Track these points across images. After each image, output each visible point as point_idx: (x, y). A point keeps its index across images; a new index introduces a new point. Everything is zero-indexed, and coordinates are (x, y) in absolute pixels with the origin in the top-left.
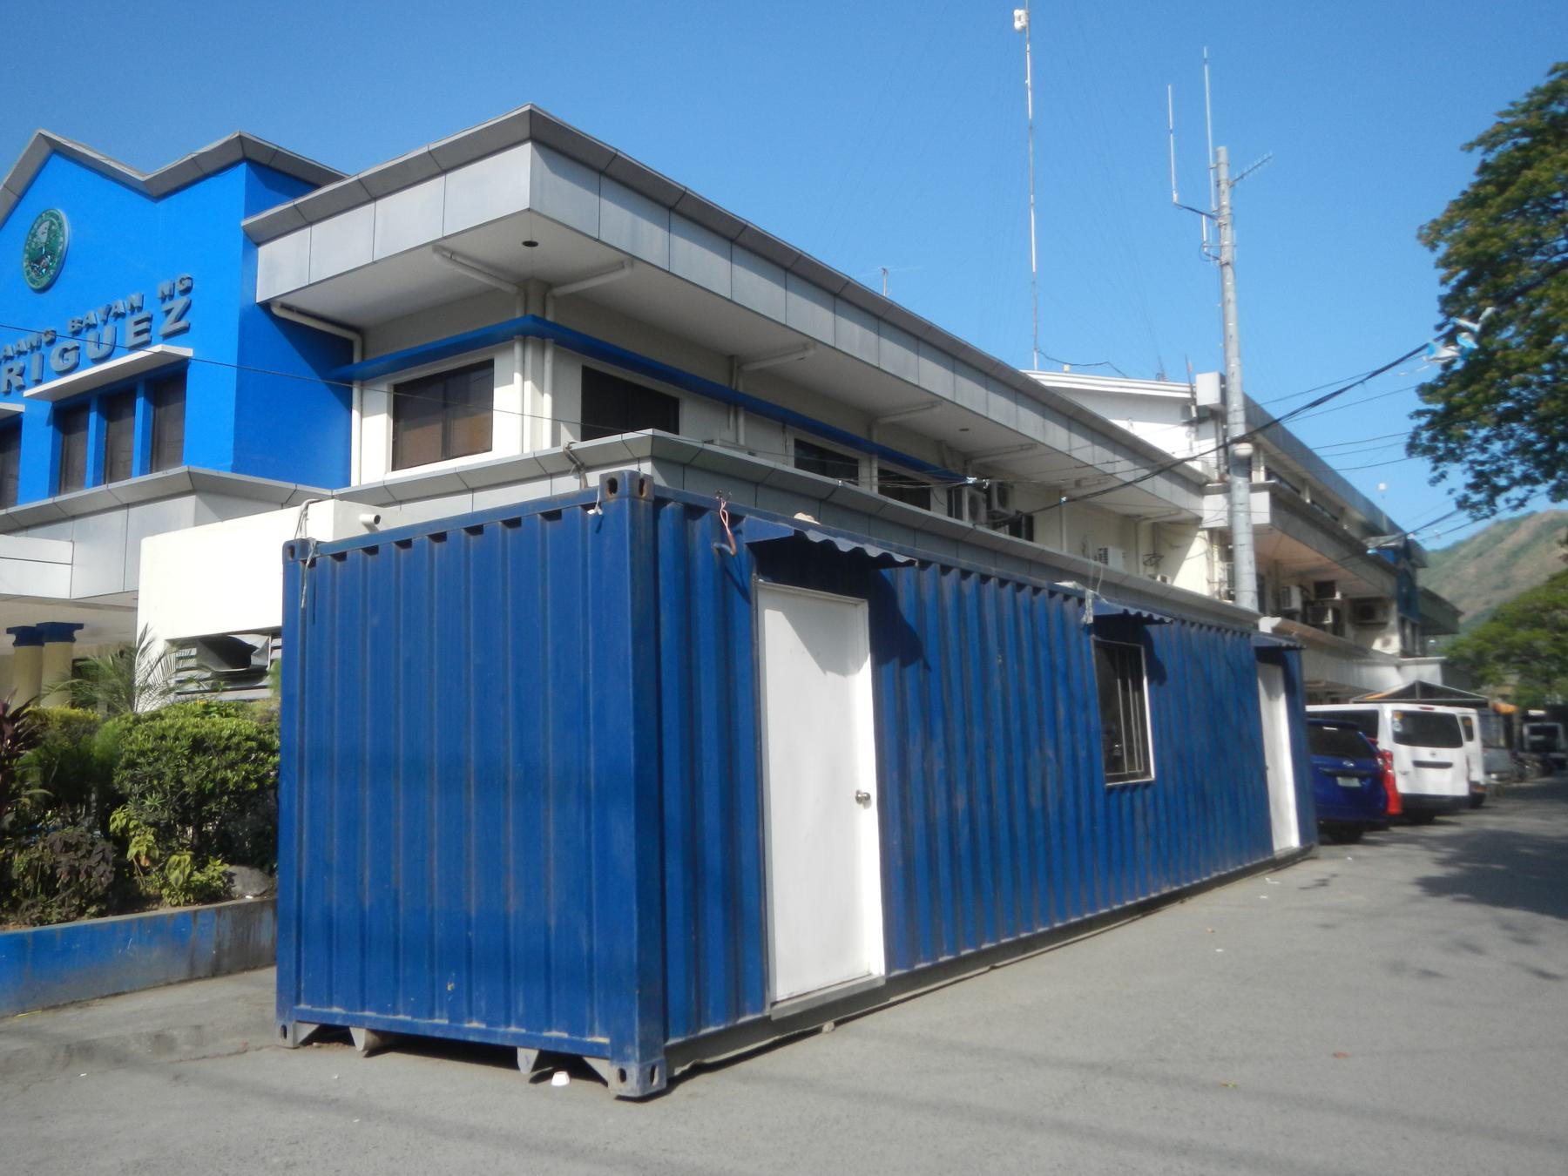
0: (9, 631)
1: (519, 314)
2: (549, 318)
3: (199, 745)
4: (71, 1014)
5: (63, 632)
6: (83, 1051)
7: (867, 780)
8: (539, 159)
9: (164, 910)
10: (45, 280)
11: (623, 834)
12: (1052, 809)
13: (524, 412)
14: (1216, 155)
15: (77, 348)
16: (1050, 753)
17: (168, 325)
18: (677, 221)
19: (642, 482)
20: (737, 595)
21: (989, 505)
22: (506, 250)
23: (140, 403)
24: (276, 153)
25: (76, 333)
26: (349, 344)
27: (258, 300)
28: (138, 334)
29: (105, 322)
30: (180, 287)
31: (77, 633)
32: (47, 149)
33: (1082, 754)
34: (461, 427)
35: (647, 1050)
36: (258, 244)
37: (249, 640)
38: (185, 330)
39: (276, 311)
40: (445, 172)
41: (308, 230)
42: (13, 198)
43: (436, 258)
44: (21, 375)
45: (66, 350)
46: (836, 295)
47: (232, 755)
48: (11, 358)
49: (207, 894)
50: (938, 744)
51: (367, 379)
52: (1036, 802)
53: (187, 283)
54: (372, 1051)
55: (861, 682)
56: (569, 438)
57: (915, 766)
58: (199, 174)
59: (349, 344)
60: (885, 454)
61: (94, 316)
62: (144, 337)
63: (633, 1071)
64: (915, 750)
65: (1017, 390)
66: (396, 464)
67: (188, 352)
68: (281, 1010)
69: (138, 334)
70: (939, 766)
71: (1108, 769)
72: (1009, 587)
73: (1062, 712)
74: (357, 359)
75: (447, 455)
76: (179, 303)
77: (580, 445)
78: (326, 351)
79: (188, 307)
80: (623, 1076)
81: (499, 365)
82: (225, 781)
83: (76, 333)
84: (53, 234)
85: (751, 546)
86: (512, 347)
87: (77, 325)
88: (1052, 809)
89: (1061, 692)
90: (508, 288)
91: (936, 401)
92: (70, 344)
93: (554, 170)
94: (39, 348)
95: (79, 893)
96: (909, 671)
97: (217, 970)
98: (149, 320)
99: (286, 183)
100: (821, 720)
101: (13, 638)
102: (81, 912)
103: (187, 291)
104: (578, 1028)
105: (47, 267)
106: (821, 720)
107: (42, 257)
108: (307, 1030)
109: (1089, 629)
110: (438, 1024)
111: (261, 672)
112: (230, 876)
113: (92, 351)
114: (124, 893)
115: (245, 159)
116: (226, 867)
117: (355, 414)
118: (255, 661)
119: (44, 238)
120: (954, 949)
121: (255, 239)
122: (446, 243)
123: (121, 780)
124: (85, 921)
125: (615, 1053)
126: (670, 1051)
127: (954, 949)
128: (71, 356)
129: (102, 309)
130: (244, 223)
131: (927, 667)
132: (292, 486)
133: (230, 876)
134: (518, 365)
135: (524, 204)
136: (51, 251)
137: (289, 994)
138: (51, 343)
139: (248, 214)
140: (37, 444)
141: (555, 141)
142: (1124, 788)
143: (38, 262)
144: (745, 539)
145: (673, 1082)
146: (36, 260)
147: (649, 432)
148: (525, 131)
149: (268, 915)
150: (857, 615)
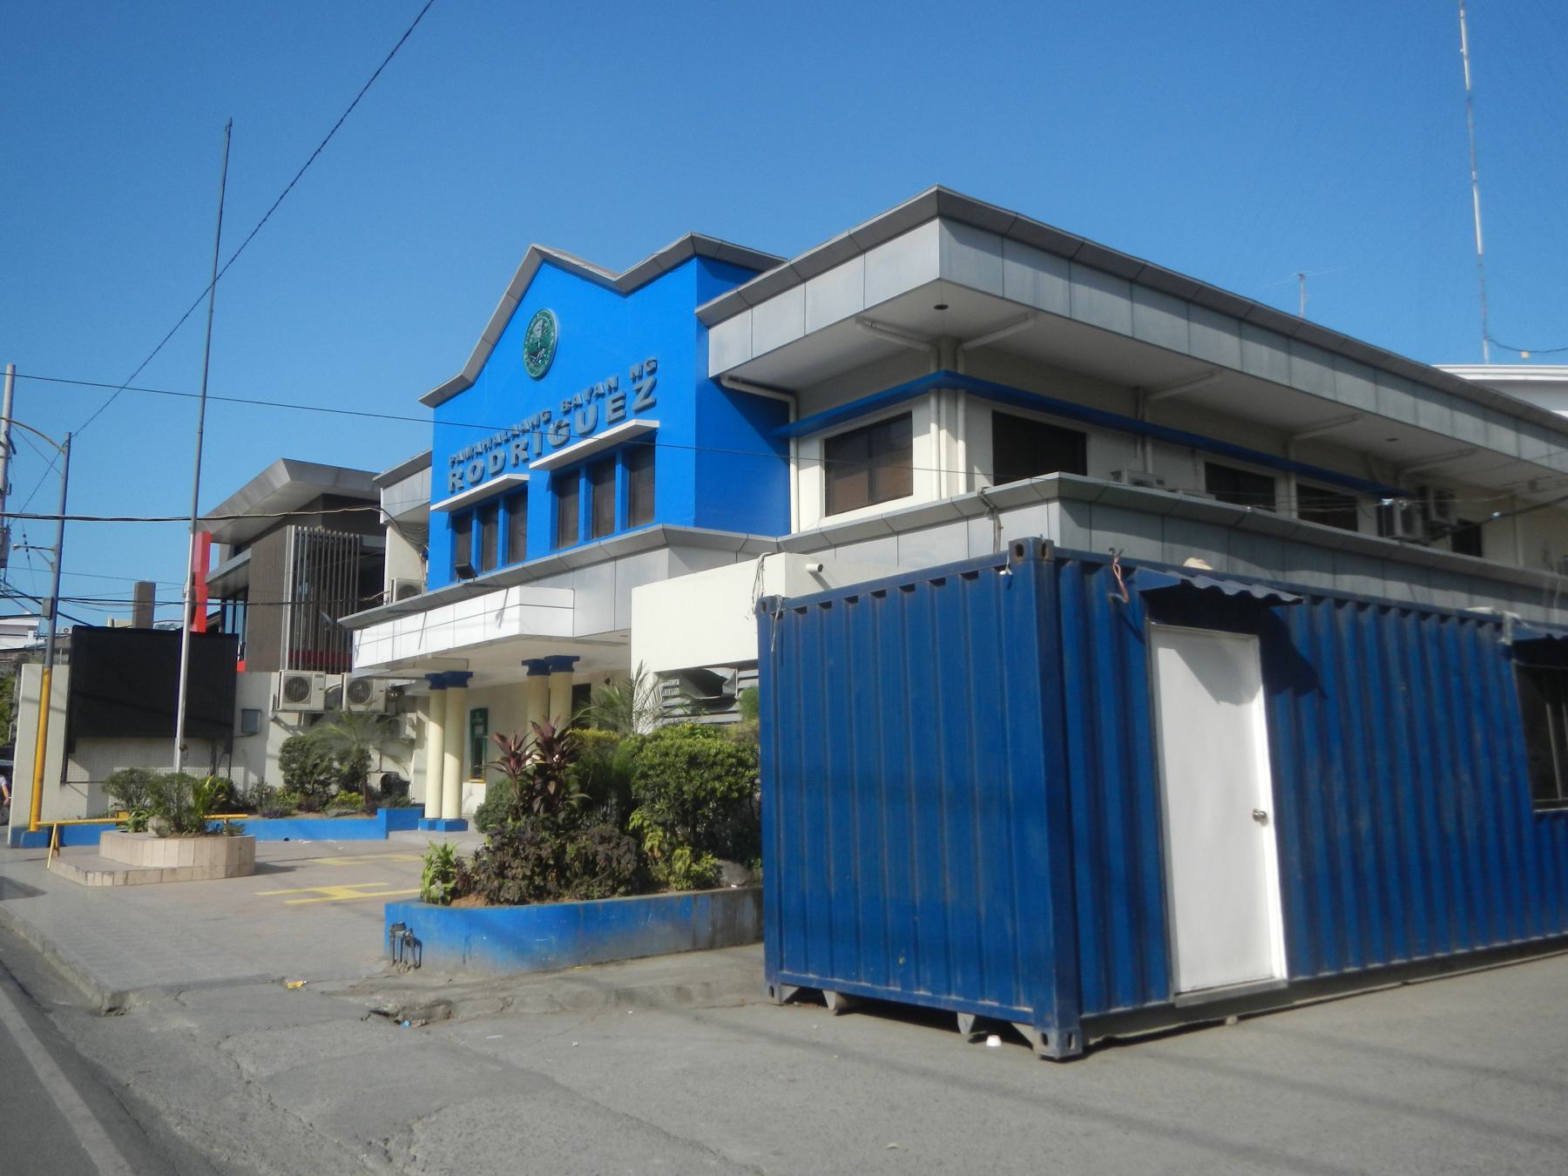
0: (524, 663)
1: (933, 370)
2: (961, 371)
3: (693, 761)
4: (612, 969)
5: (564, 664)
6: (626, 996)
7: (1265, 801)
9: (672, 893)
10: (541, 370)
11: (1038, 839)
12: (1470, 832)
13: (940, 459)
16: (1466, 778)
17: (639, 402)
18: (1076, 269)
19: (1044, 546)
20: (1132, 638)
21: (1425, 512)
22: (922, 314)
23: (619, 468)
24: (721, 247)
26: (785, 405)
27: (711, 374)
28: (615, 410)
30: (646, 369)
31: (575, 664)
32: (538, 259)
33: (1505, 780)
34: (884, 474)
35: (1064, 1022)
36: (709, 327)
37: (720, 672)
38: (653, 405)
39: (725, 383)
40: (864, 251)
42: (515, 302)
43: (859, 327)
46: (1241, 320)
47: (718, 770)
49: (701, 882)
50: (1337, 767)
51: (802, 436)
52: (1450, 827)
53: (653, 365)
54: (842, 1011)
55: (1256, 711)
56: (983, 482)
57: (1313, 787)
59: (785, 405)
60: (1302, 470)
61: (580, 397)
62: (620, 413)
63: (1053, 1036)
64: (1313, 773)
65: (1450, 394)
66: (830, 510)
67: (655, 424)
68: (768, 975)
69: (615, 410)
70: (1338, 788)
71: (1536, 795)
72: (1411, 618)
73: (1479, 737)
74: (792, 420)
75: (873, 500)
76: (647, 382)
77: (993, 489)
78: (767, 413)
80: (1045, 1040)
81: (917, 417)
82: (714, 790)
83: (567, 412)
84: (546, 331)
85: (1144, 594)
86: (927, 401)
88: (1470, 832)
89: (1477, 719)
90: (923, 347)
91: (1356, 414)
93: (961, 240)
95: (612, 875)
96: (1306, 701)
97: (711, 946)
98: (623, 398)
99: (731, 272)
100: (1217, 749)
101: (526, 668)
102: (614, 891)
103: (653, 372)
104: (1006, 998)
106: (1217, 749)
108: (790, 991)
109: (1508, 652)
110: (893, 990)
111: (730, 700)
112: (719, 868)
113: (580, 427)
114: (642, 881)
115: (696, 255)
116: (716, 861)
117: (793, 467)
118: (726, 690)
120: (1362, 961)
121: (706, 323)
122: (870, 314)
123: (636, 786)
124: (616, 898)
125: (1038, 1021)
126: (1085, 1024)
127: (1362, 961)
128: (563, 431)
129: (587, 390)
131: (1323, 696)
132: (743, 536)
133: (719, 868)
134: (933, 416)
135: (934, 273)
136: (545, 346)
137: (775, 963)
138: (548, 421)
139: (700, 302)
140: (540, 505)
141: (962, 216)
142: (1557, 816)
143: (535, 354)
144: (1137, 588)
145: (1088, 1051)
146: (533, 354)
147: (1055, 475)
148: (933, 209)
149: (749, 903)
150: (1247, 654)
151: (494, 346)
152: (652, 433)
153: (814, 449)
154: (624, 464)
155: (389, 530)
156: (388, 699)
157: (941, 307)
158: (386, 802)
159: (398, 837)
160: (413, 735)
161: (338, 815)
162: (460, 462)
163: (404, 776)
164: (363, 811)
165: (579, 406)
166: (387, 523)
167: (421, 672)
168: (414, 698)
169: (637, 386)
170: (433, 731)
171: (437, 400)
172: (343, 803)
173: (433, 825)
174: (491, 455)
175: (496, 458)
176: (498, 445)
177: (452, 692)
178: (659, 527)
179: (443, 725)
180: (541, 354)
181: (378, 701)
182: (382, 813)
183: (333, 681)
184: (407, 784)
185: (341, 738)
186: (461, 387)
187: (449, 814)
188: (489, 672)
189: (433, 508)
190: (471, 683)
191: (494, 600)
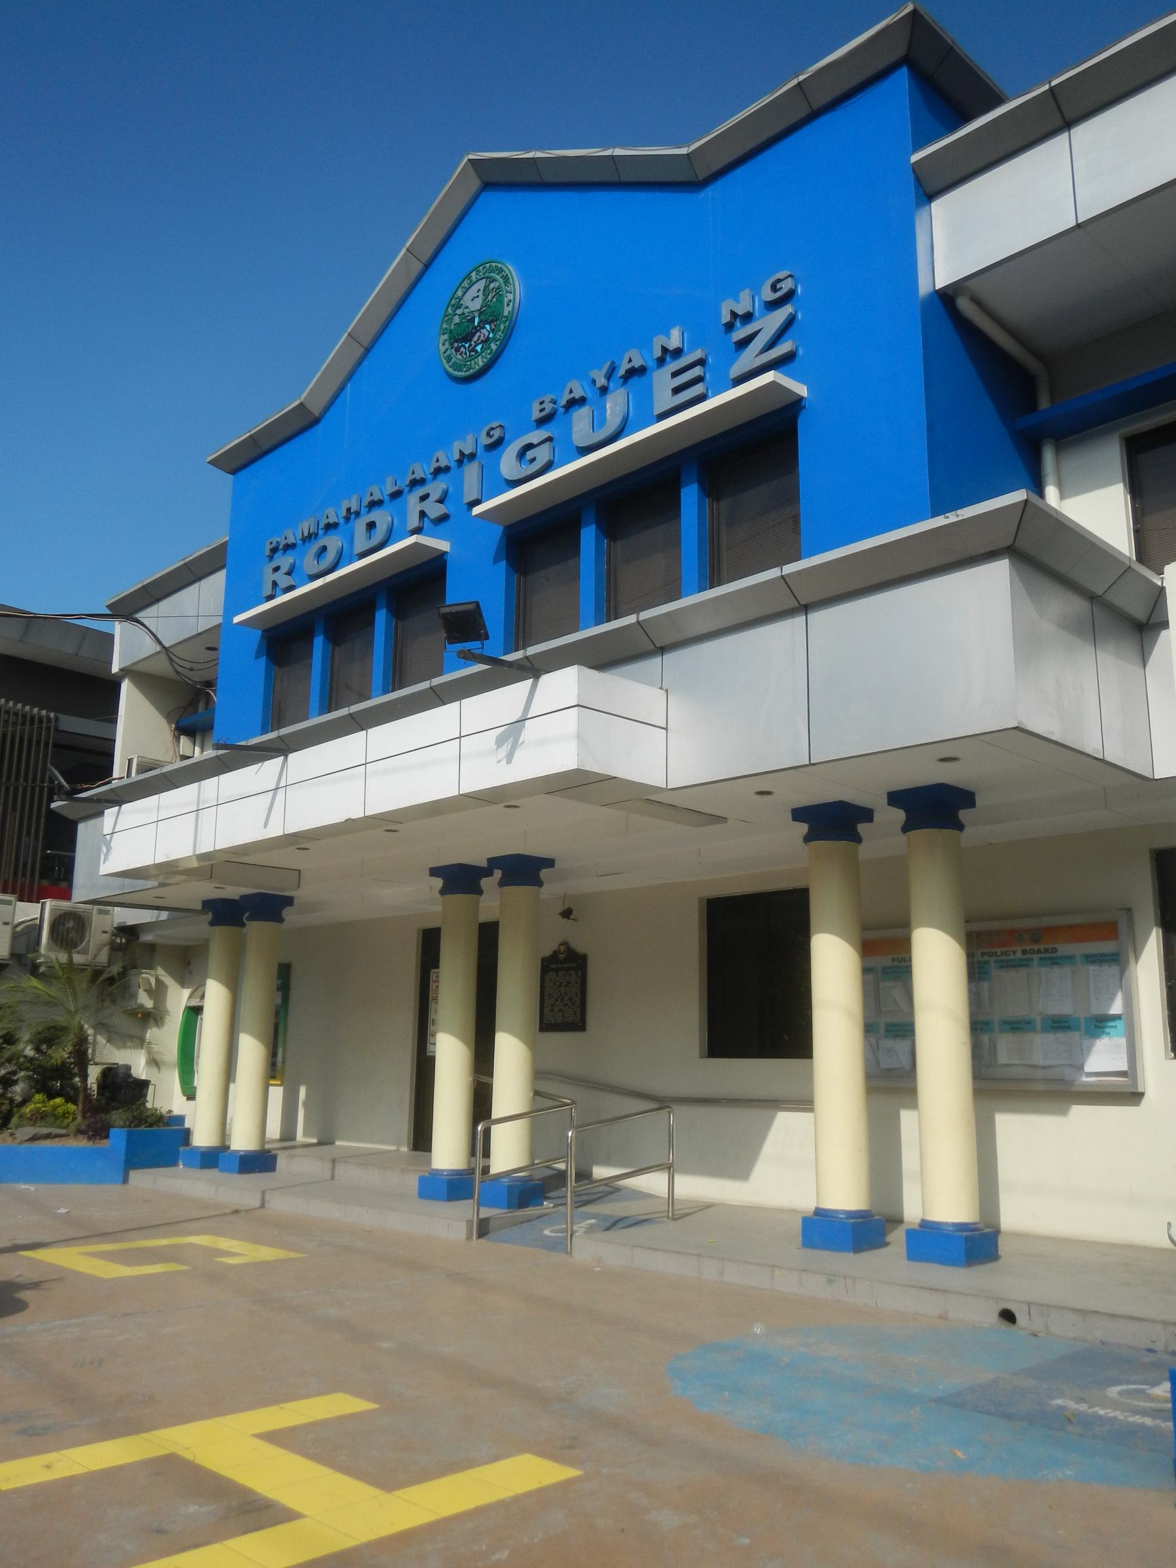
0: (434, 872)
5: (523, 870)
10: (481, 362)
15: (550, 439)
24: (949, 54)
25: (542, 422)
28: (676, 391)
29: (604, 390)
31: (544, 873)
32: (475, 183)
36: (931, 197)
39: (964, 305)
42: (417, 267)
44: (441, 501)
45: (530, 446)
48: (422, 482)
51: (1077, 431)
53: (786, 286)
67: (802, 390)
69: (676, 391)
74: (1044, 403)
79: (790, 321)
84: (493, 297)
87: (548, 407)
92: (535, 436)
94: (472, 456)
98: (701, 362)
101: (438, 883)
103: (789, 296)
105: (487, 341)
107: (476, 330)
119: (476, 305)
121: (931, 186)
128: (542, 455)
130: (914, 158)
138: (496, 445)
139: (917, 147)
143: (467, 338)
146: (462, 337)
151: (368, 350)
152: (795, 405)
153: (1110, 454)
155: (126, 686)
156: (114, 948)
158: (117, 1116)
159: (141, 1179)
160: (149, 1004)
161: (34, 1138)
162: (289, 547)
163: (140, 1070)
164: (80, 1132)
165: (582, 401)
166: (125, 672)
167: (209, 890)
168: (152, 947)
169: (740, 333)
170: (215, 995)
171: (239, 461)
172: (39, 1117)
173: (212, 1158)
174: (360, 525)
175: (371, 526)
176: (374, 504)
177: (256, 931)
179: (234, 985)
180: (479, 343)
181: (95, 947)
182: (118, 1137)
183: (27, 911)
184: (145, 1084)
185: (51, 1003)
186: (302, 423)
187: (243, 1140)
188: (323, 896)
189: (237, 619)
190: (287, 913)
191: (505, 701)
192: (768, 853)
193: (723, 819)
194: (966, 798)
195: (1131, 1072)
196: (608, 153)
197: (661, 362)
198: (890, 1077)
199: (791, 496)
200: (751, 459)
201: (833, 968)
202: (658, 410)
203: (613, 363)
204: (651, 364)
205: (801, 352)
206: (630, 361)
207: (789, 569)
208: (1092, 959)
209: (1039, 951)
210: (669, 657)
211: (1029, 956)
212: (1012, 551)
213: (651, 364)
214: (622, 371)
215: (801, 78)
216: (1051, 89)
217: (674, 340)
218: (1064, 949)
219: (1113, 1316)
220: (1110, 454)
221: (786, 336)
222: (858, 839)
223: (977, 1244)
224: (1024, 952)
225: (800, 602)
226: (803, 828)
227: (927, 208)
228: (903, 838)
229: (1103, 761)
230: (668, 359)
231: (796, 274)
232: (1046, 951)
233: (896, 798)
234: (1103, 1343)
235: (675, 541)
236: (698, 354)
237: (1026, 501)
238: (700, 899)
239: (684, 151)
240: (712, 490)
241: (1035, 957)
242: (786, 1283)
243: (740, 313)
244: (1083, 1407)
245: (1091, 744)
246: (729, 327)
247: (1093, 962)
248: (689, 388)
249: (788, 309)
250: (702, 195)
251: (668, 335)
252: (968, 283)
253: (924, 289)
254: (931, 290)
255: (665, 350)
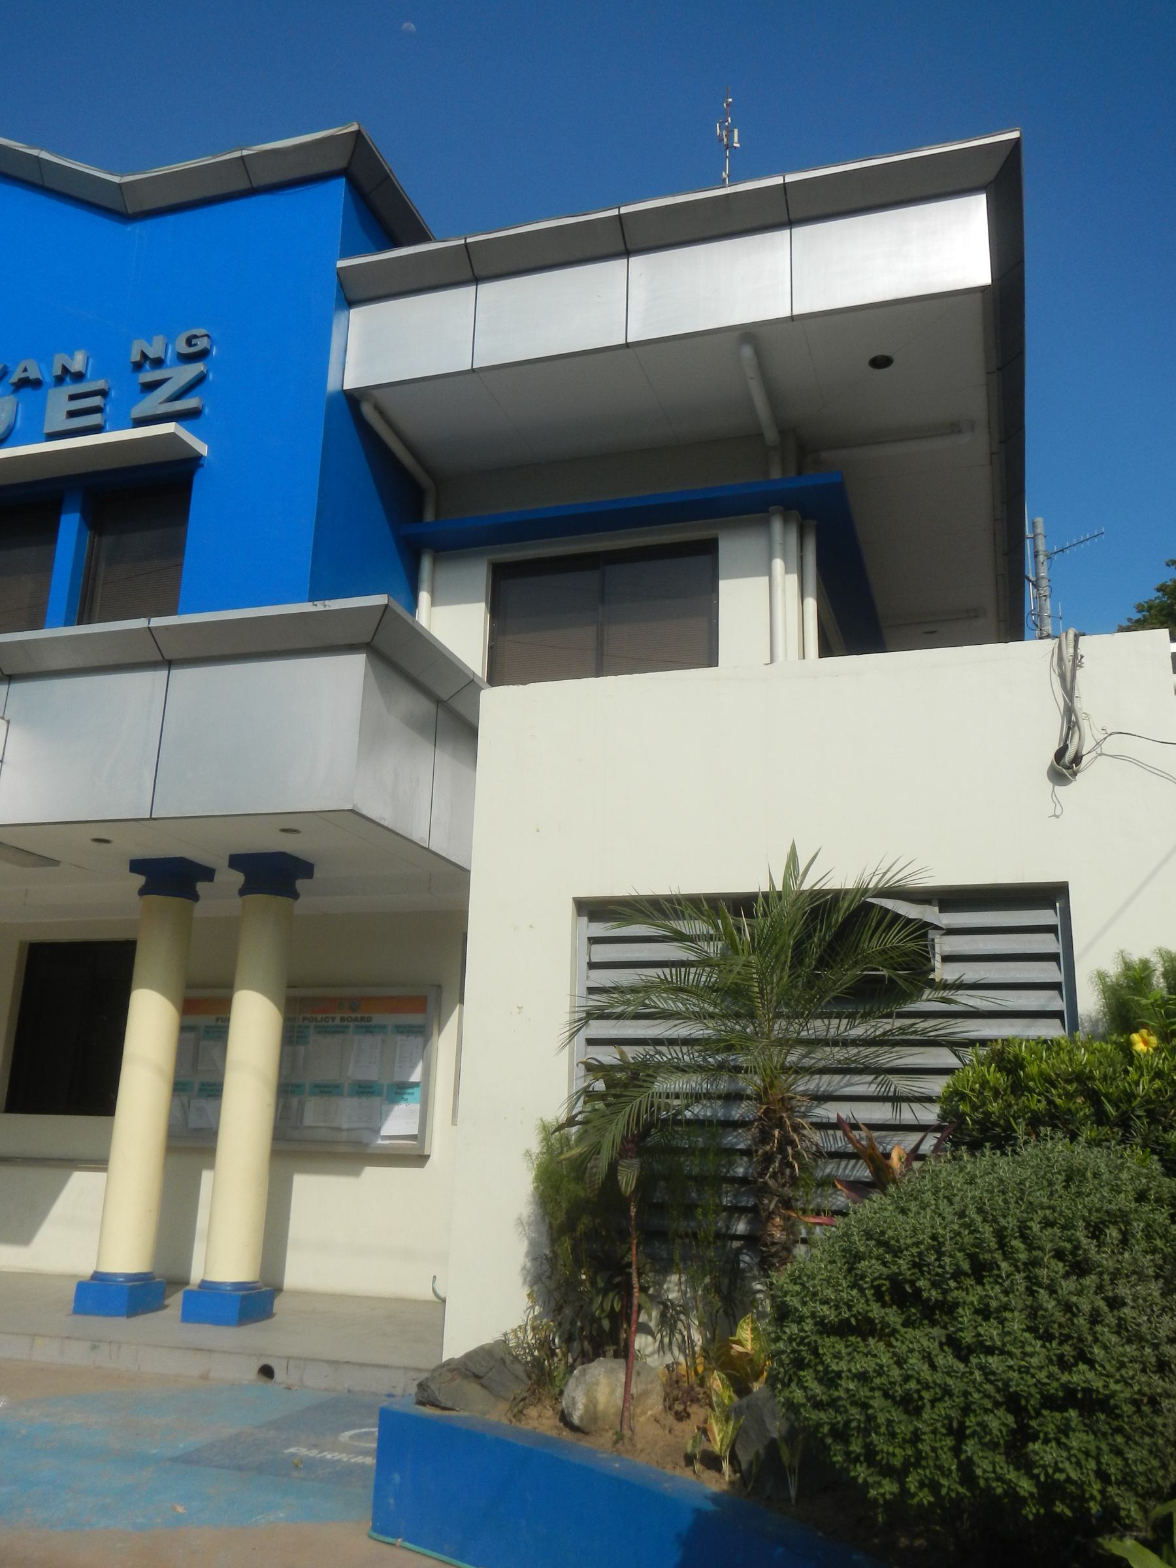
8: (185, 423)
14: (1034, 525)
24: (385, 180)
28: (72, 414)
36: (351, 304)
39: (367, 409)
41: (465, 294)
43: (747, 352)
51: (452, 546)
53: (202, 344)
58: (243, 185)
62: (94, 419)
67: (203, 449)
69: (72, 414)
74: (429, 516)
79: (200, 379)
81: (730, 548)
86: (766, 524)
90: (771, 435)
98: (103, 393)
103: (202, 355)
117: (424, 597)
121: (353, 293)
130: (341, 264)
139: (344, 255)
148: (991, 170)
152: (195, 460)
153: (478, 574)
154: (85, 517)
157: (881, 363)
169: (149, 376)
178: (380, 600)
192: (101, 902)
193: (54, 862)
194: (305, 868)
195: (420, 1137)
196: (34, 152)
197: (60, 380)
198: (191, 1137)
199: (175, 550)
200: (140, 504)
201: (150, 1024)
202: (48, 429)
203: (5, 367)
204: (48, 379)
205: (206, 411)
206: (25, 370)
207: (157, 622)
208: (402, 1030)
209: (356, 1019)
210: (17, 688)
211: (346, 1023)
212: (369, 647)
213: (48, 379)
214: (14, 378)
215: (245, 153)
216: (466, 245)
217: (77, 363)
218: (378, 1018)
219: (362, 1365)
220: (478, 574)
221: (194, 392)
222: (195, 897)
223: (254, 1302)
224: (342, 1019)
225: (164, 657)
226: (140, 880)
227: (346, 313)
228: (238, 901)
229: (428, 849)
230: (68, 379)
231: (214, 335)
232: (362, 1019)
233: (237, 861)
234: (349, 1391)
235: (46, 567)
236: (100, 384)
237: (386, 606)
238: (21, 943)
239: (116, 179)
240: (95, 522)
241: (352, 1024)
242: (47, 1352)
243: (151, 355)
244: (313, 1453)
245: (419, 833)
246: (138, 367)
247: (402, 1033)
248: (86, 415)
249: (198, 368)
250: (129, 228)
251: (72, 356)
252: (375, 392)
253: (332, 385)
254: (338, 388)
255: (65, 370)
